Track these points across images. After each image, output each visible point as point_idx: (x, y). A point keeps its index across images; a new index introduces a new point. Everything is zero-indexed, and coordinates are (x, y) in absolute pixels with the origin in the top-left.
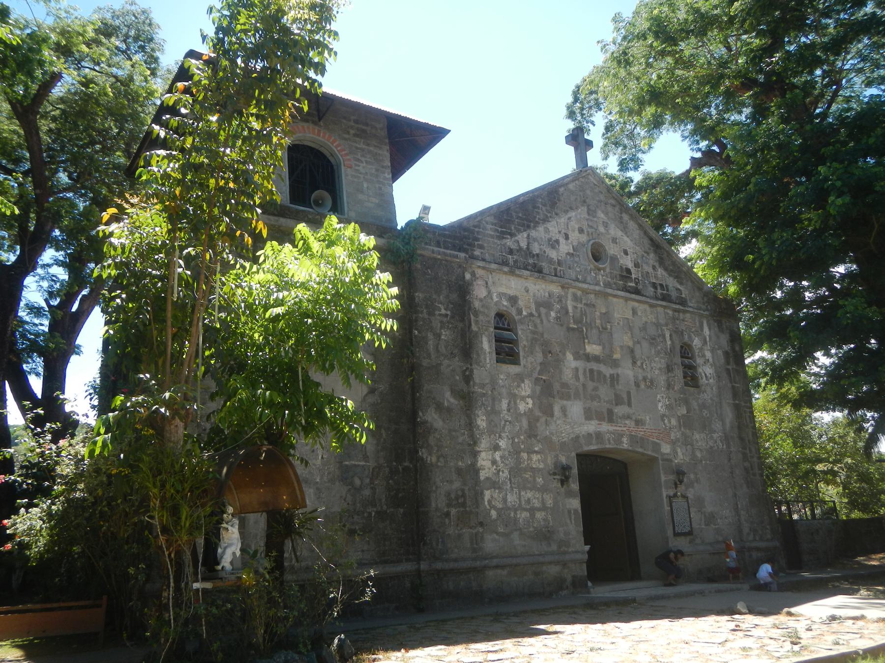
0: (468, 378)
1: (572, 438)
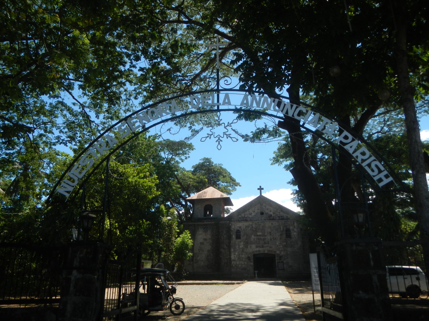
0: (230, 243)
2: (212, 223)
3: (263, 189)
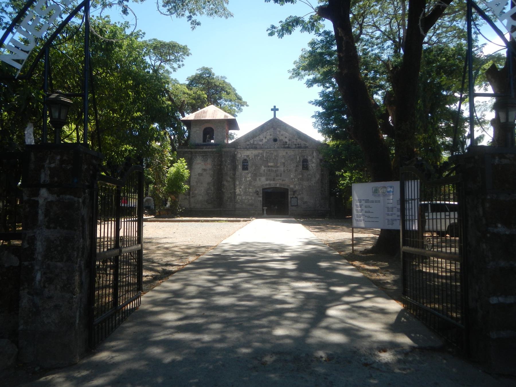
0: (234, 174)
2: (213, 150)
3: (278, 110)
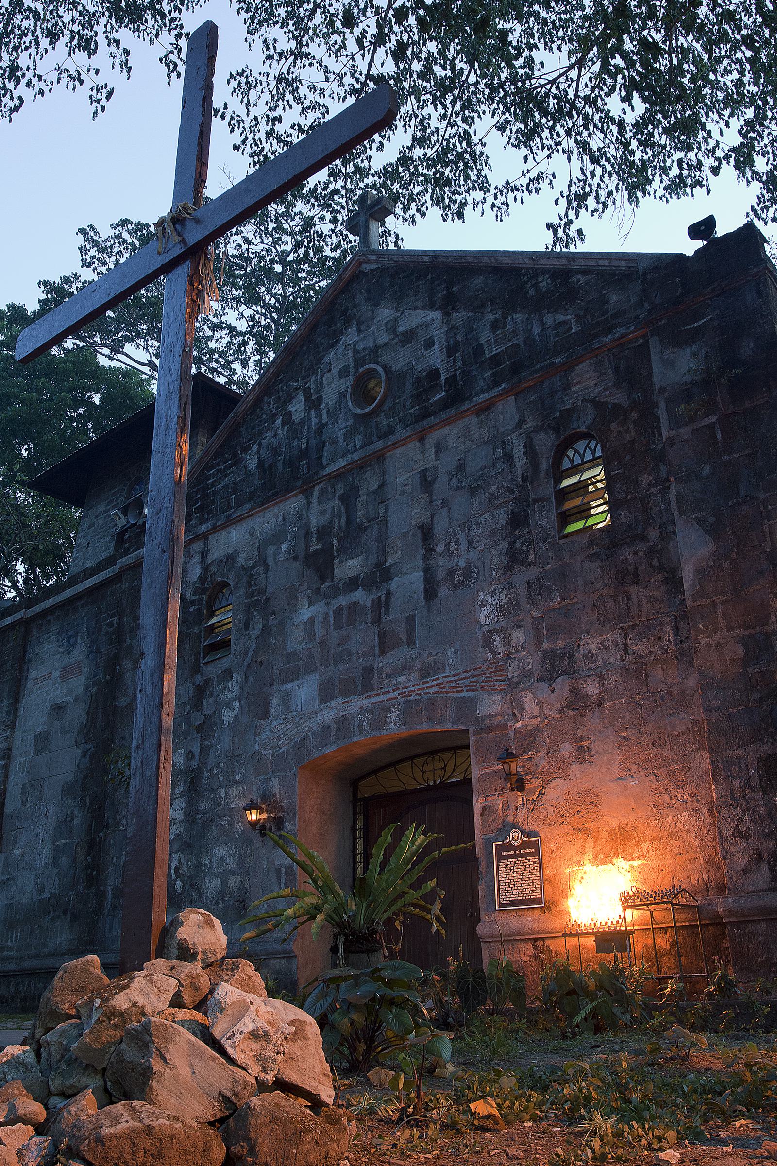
1: (296, 743)
